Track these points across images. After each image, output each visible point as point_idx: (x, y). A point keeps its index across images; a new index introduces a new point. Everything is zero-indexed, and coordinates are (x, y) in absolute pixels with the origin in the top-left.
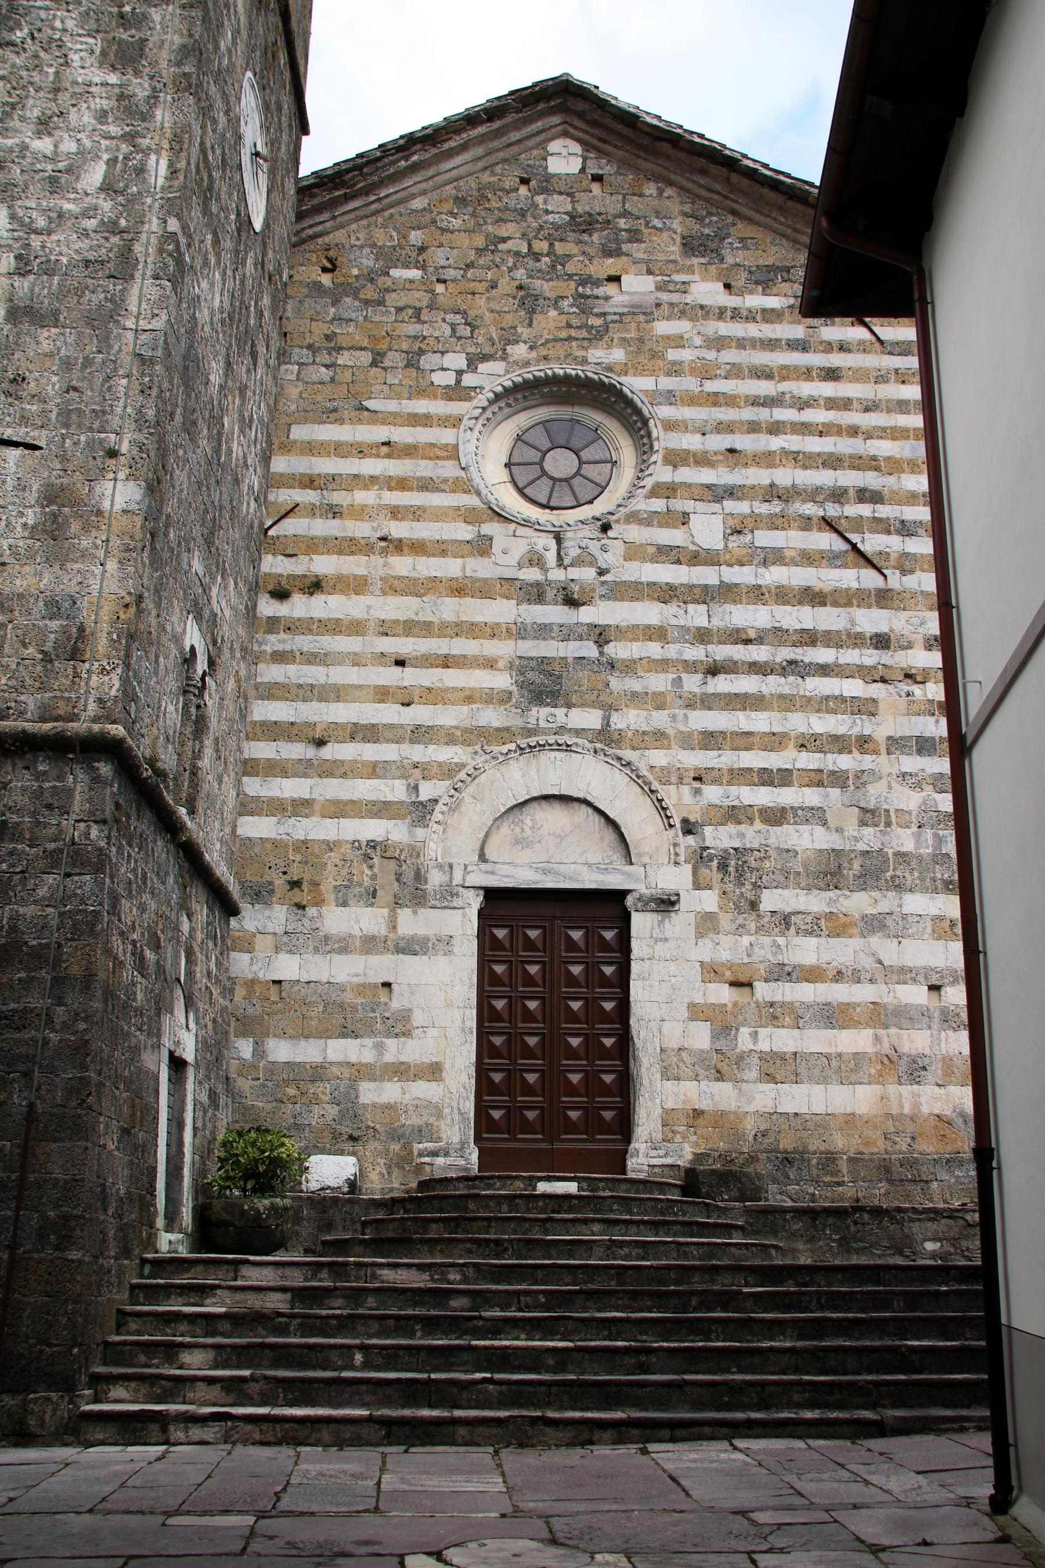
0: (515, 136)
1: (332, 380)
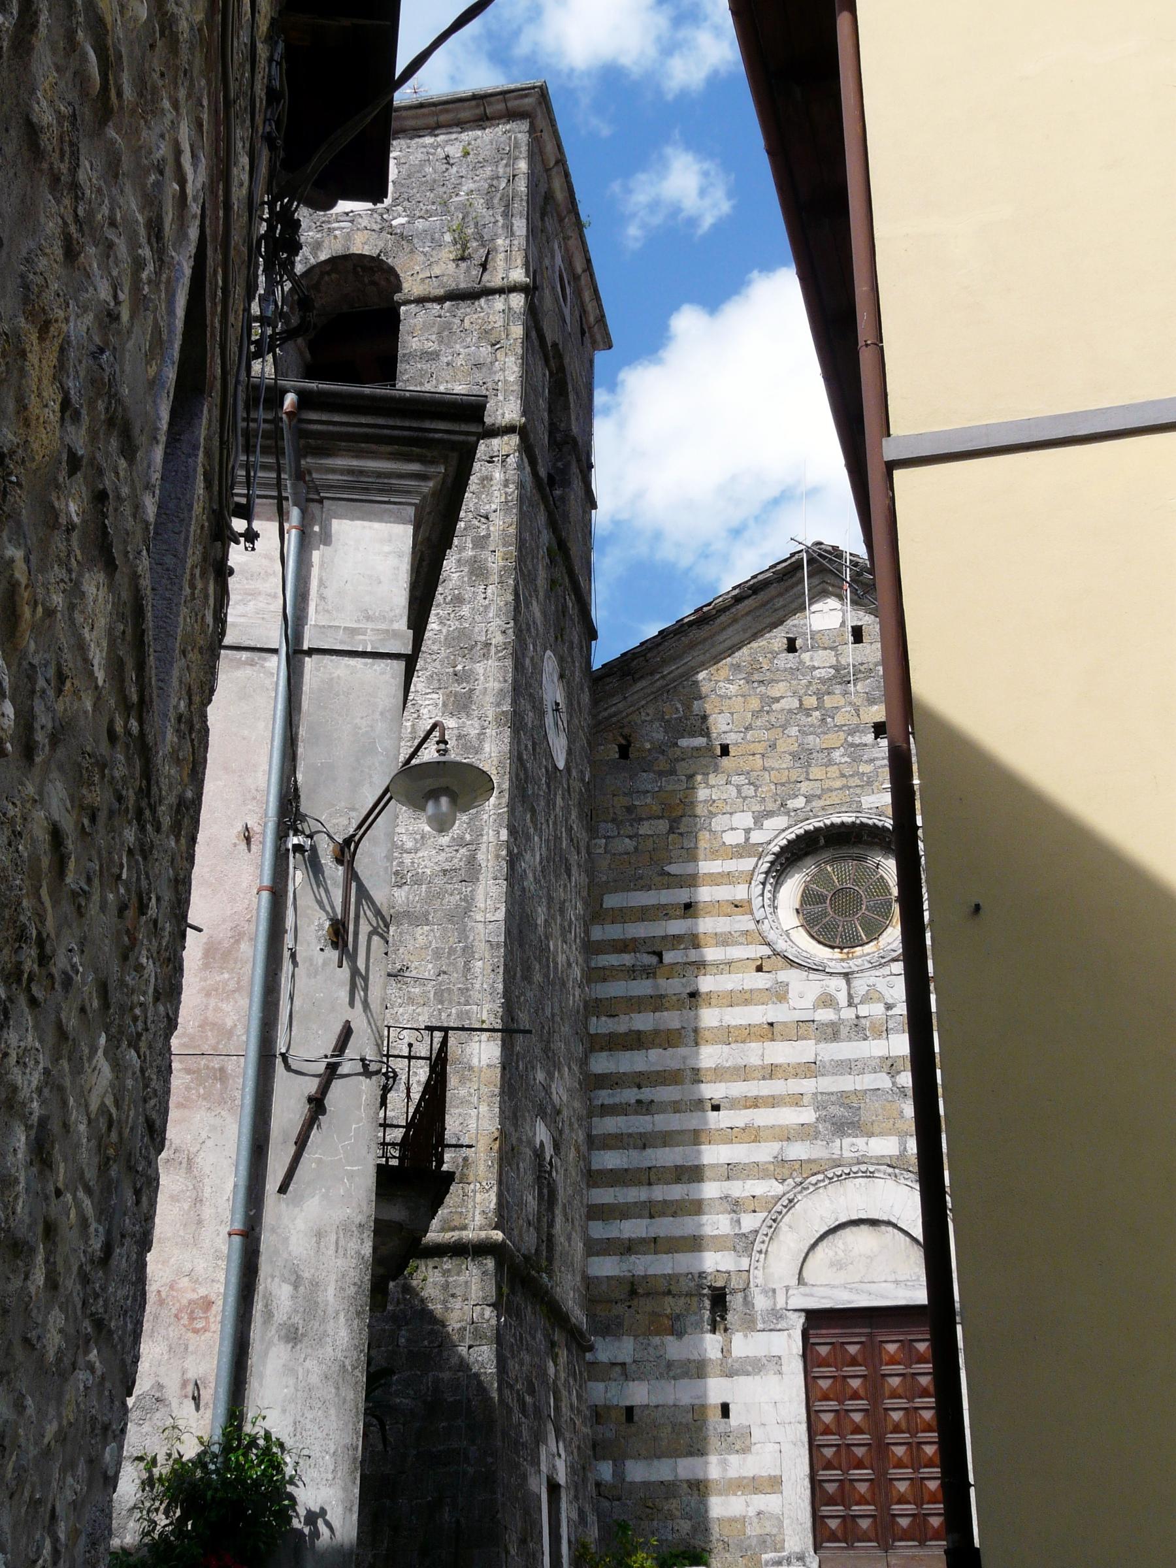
0: (780, 602)
1: (636, 848)
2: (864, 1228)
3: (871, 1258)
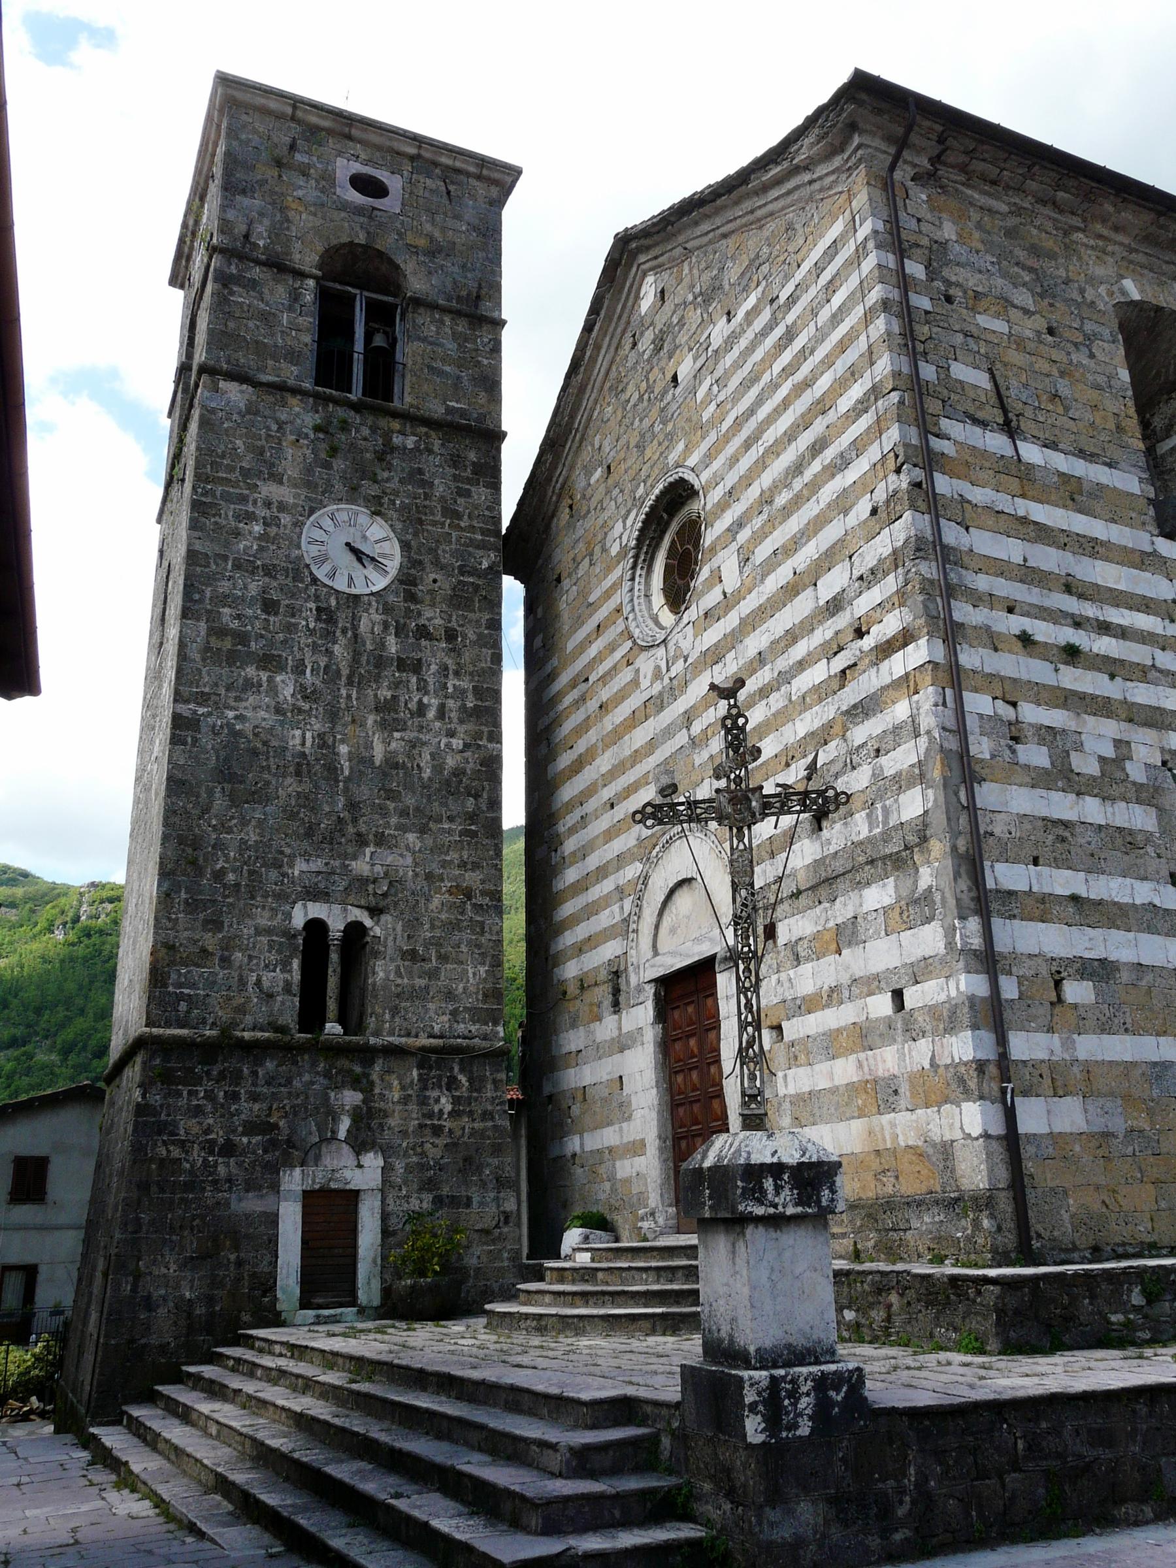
2: (685, 888)
3: (688, 917)
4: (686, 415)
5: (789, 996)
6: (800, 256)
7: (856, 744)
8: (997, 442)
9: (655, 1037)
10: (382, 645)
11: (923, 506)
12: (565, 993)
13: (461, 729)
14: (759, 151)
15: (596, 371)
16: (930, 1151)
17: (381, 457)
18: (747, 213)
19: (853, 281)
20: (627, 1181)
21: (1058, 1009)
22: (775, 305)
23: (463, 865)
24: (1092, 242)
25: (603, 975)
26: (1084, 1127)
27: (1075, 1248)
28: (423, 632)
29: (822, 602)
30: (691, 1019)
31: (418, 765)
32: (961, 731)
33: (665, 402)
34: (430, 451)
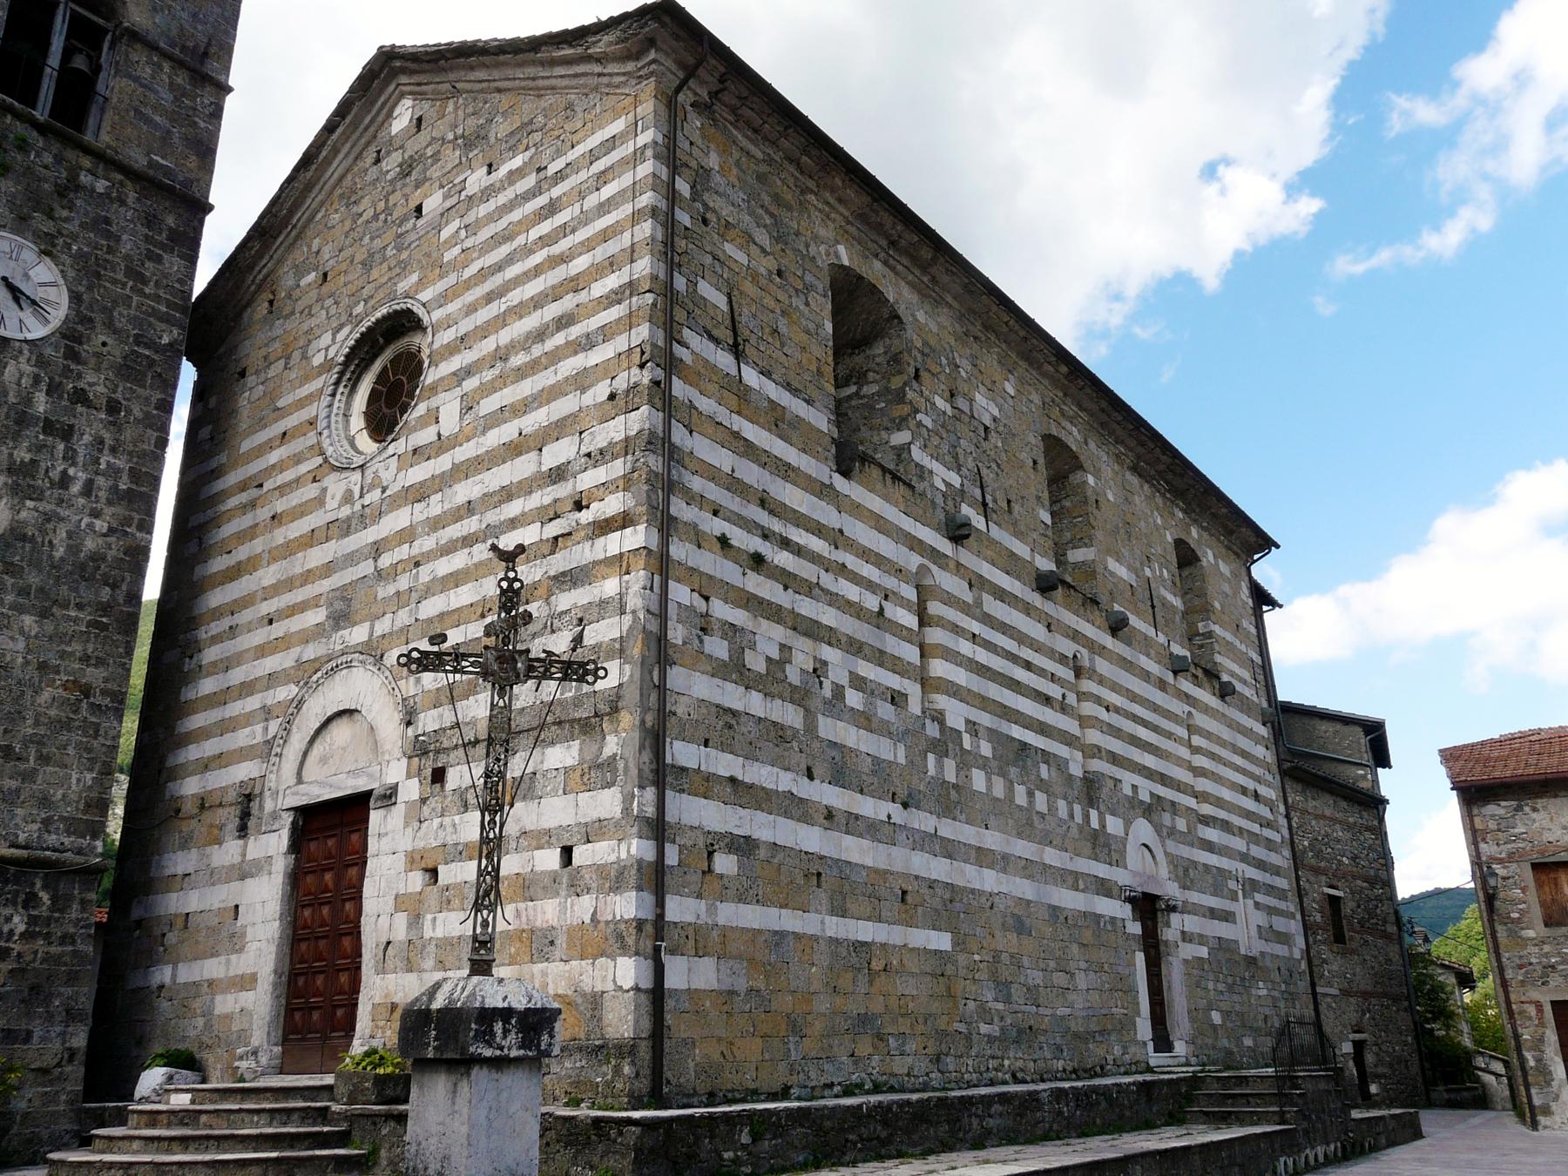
2: (345, 719)
3: (344, 749)
4: (425, 248)
5: (450, 840)
6: (575, 138)
7: (559, 609)
8: (724, 360)
9: (287, 867)
10: (28, 400)
11: (659, 405)
12: (178, 811)
13: (109, 511)
14: (556, 26)
15: (329, 173)
16: (579, 1000)
17: (62, 192)
18: (528, 78)
19: (626, 180)
20: (228, 1017)
21: (708, 877)
22: (542, 174)
23: (85, 659)
24: (820, 206)
25: (232, 796)
26: (715, 986)
27: (695, 1093)
28: (80, 397)
29: (544, 468)
30: (330, 853)
31: (50, 542)
32: (662, 616)
33: (404, 229)
34: (123, 203)
